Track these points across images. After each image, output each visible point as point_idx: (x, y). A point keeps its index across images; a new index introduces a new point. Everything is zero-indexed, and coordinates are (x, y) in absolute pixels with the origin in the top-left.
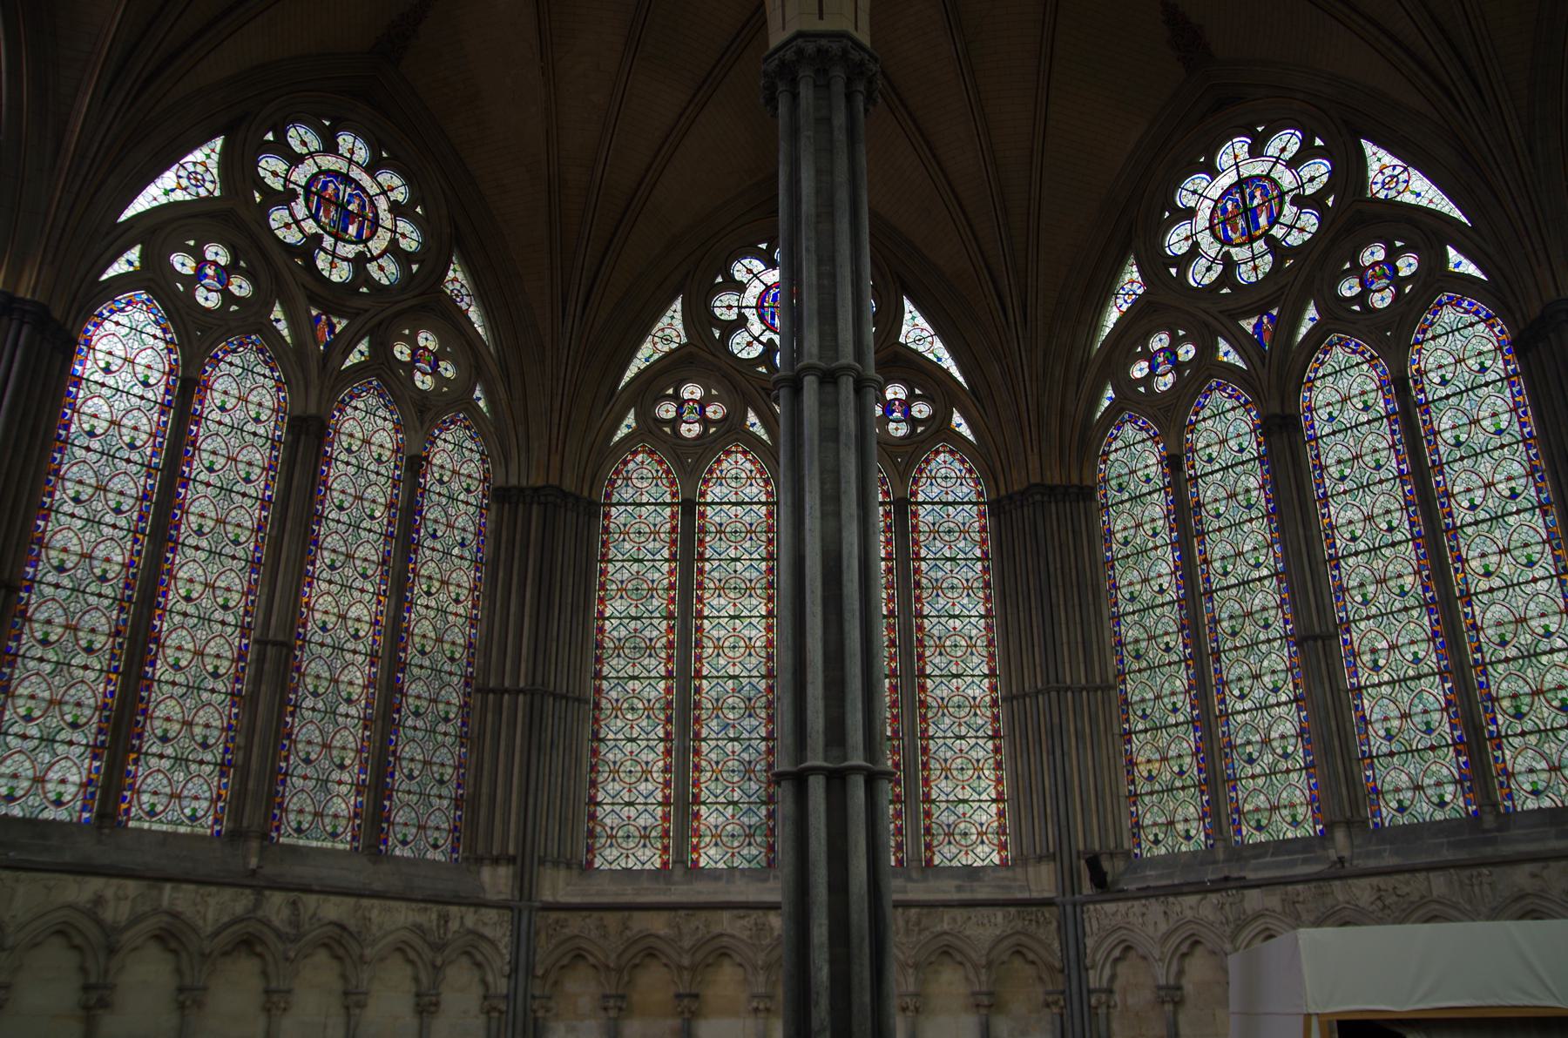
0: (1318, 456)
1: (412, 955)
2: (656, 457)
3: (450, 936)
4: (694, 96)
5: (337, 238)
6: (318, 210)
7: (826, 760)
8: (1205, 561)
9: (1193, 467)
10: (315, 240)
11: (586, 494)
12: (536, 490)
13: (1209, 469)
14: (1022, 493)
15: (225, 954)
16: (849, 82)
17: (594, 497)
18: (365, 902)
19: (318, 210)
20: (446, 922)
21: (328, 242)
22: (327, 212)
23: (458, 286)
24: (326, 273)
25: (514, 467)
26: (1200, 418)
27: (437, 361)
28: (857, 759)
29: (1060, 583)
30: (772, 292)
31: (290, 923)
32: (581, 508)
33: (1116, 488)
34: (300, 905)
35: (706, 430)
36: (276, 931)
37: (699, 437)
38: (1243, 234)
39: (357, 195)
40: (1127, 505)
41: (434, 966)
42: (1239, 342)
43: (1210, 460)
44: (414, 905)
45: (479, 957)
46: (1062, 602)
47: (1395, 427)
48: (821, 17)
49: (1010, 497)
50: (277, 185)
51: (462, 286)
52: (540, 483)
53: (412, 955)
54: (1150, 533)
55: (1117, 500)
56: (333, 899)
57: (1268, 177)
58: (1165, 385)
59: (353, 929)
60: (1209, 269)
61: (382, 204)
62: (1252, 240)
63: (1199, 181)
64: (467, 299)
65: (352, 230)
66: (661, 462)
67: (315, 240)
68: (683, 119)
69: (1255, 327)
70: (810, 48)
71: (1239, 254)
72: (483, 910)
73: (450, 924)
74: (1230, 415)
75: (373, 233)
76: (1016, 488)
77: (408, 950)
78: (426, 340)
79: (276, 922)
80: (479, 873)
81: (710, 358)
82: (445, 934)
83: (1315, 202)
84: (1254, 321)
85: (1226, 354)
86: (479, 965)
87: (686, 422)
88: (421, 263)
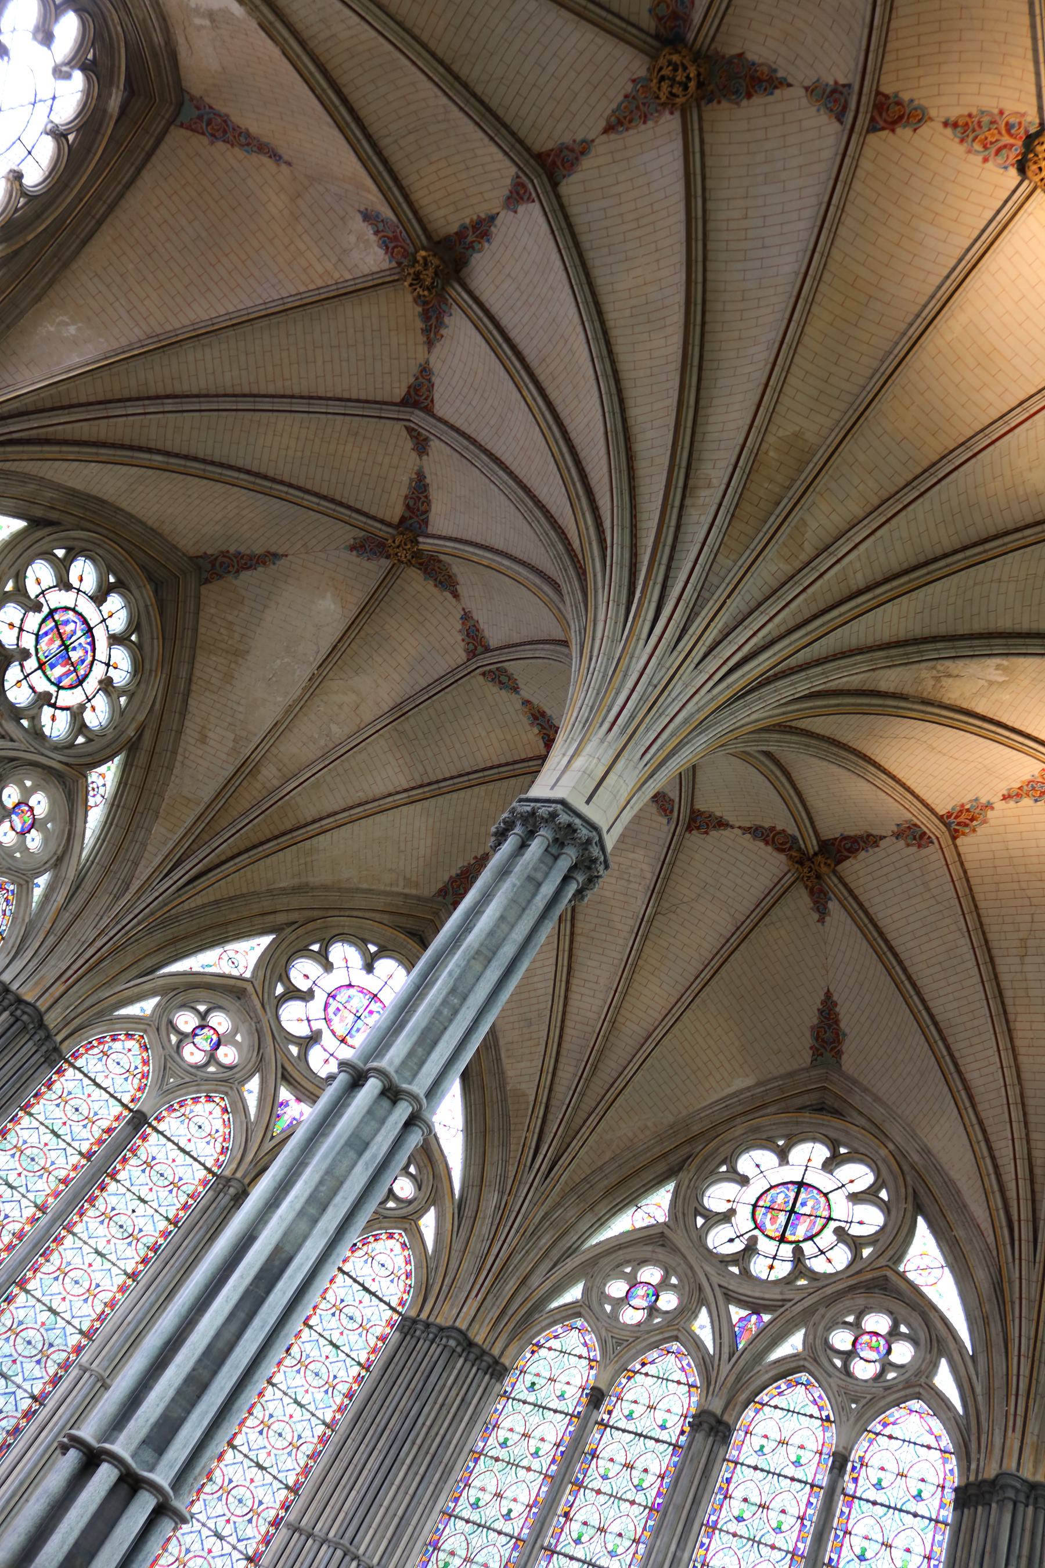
0: (729, 1481)
2: (145, 1055)
4: (413, 788)
5: (41, 666)
6: (46, 634)
7: (133, 1456)
8: (566, 1515)
9: (610, 1413)
10: (25, 654)
11: (59, 1038)
12: (19, 1001)
13: (622, 1424)
14: (441, 1329)
16: (574, 868)
17: (64, 1047)
19: (46, 634)
21: (31, 664)
22: (52, 641)
23: (100, 782)
25: (18, 965)
26: (644, 1370)
27: (32, 826)
28: (162, 1477)
29: (419, 1441)
32: (44, 1048)
33: (528, 1385)
35: (207, 1064)
37: (197, 1067)
38: (777, 1230)
39: (85, 648)
40: (529, 1408)
42: (720, 1322)
43: (629, 1417)
46: (408, 1461)
47: (813, 1500)
48: (588, 802)
49: (428, 1325)
50: (33, 590)
51: (104, 785)
52: (29, 998)
54: (532, 1450)
55: (521, 1396)
57: (826, 1195)
58: (632, 1318)
60: (731, 1240)
61: (98, 671)
62: (782, 1239)
63: (766, 1158)
64: (98, 798)
65: (58, 671)
66: (145, 1063)
67: (25, 654)
68: (390, 799)
69: (741, 1319)
70: (564, 818)
71: (765, 1245)
74: (672, 1386)
76: (438, 1321)
78: (40, 804)
81: (259, 1006)
83: (855, 1244)
84: (744, 1313)
85: (702, 1327)
87: (195, 1045)
88: (89, 740)
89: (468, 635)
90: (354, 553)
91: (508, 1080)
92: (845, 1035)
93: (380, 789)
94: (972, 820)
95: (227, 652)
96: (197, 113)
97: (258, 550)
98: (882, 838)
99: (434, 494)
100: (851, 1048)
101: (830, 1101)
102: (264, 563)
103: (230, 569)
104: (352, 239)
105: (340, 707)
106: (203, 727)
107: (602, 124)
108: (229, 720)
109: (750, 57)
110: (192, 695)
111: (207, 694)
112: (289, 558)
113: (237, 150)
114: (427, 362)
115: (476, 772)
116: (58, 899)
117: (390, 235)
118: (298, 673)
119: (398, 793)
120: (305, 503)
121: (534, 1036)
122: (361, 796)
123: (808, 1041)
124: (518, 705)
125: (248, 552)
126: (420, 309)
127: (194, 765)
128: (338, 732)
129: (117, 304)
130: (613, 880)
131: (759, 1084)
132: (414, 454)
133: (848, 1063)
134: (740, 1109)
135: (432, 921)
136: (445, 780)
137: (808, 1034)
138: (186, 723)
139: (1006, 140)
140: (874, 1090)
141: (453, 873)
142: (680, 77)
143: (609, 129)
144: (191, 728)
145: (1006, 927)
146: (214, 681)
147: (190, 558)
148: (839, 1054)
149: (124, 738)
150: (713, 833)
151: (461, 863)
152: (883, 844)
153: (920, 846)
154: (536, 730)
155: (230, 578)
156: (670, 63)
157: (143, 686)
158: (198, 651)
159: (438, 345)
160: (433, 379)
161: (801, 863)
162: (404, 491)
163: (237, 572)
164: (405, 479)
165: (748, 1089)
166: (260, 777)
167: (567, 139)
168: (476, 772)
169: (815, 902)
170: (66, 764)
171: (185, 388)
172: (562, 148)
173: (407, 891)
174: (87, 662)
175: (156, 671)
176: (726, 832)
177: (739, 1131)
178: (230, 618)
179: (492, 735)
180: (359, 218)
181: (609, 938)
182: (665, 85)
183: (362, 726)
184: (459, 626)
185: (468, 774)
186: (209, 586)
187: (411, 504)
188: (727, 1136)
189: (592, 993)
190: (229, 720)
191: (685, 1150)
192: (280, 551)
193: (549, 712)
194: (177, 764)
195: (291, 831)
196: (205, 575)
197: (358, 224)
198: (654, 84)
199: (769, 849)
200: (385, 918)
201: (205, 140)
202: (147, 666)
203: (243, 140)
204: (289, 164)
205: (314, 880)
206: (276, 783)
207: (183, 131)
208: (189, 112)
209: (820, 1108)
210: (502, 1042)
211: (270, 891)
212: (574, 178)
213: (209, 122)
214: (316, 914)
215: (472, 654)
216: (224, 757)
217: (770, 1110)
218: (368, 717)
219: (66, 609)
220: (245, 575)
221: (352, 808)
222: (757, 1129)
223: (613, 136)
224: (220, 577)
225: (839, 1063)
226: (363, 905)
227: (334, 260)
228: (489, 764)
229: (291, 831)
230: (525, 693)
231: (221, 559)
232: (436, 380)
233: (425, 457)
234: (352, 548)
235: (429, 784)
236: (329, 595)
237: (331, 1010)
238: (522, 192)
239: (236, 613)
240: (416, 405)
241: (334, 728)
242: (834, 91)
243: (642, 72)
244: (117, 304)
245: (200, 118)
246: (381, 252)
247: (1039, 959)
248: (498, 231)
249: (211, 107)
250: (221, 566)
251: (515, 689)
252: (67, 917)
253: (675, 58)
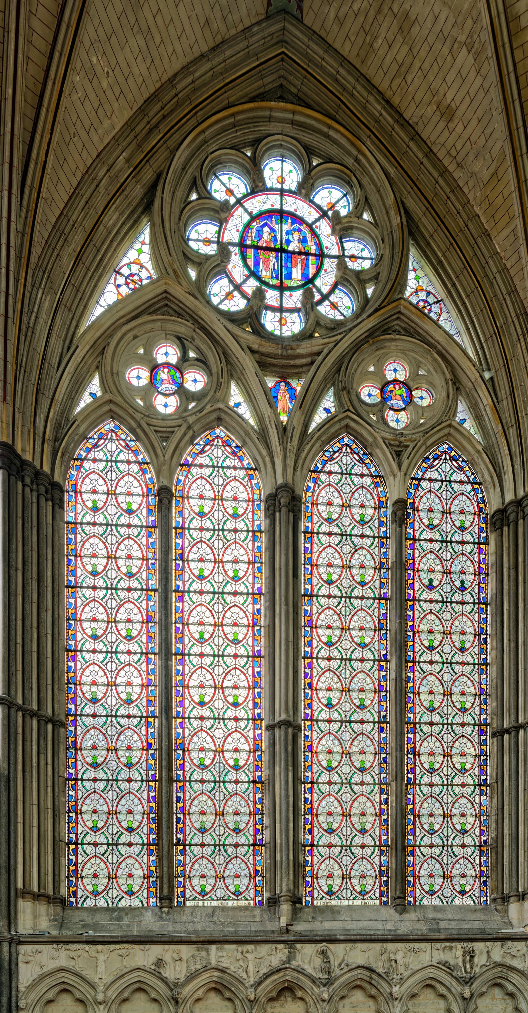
1: (442, 990)
3: (477, 970)
5: (281, 288)
6: (257, 264)
15: (271, 1000)
18: (391, 946)
19: (257, 264)
20: (472, 957)
21: (272, 297)
22: (267, 261)
24: (277, 333)
25: (508, 479)
31: (322, 970)
34: (329, 953)
36: (309, 977)
39: (294, 230)
41: (464, 999)
44: (438, 945)
45: (510, 988)
53: (442, 990)
56: (360, 946)
59: (381, 971)
72: (510, 944)
73: (476, 959)
75: (319, 269)
77: (438, 986)
79: (309, 970)
80: (506, 911)
82: (472, 968)
86: (511, 995)
116: (485, 403)
147: (267, 18)
149: (397, 232)
157: (365, 181)
170: (376, 310)
174: (308, 236)
175: (359, 151)
202: (350, 161)
219: (247, 227)
252: (506, 404)
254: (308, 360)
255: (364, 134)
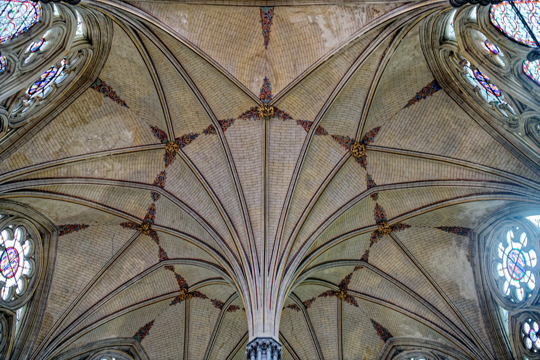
4: (99, 204)
30: (13, 250)
68: (91, 203)
89: (159, 178)
90: (151, 129)
91: (47, 308)
92: (148, 334)
93: (88, 197)
94: (233, 309)
95: (80, 117)
96: (267, 12)
97: (122, 98)
98: (207, 298)
99: (194, 142)
100: (147, 338)
101: (132, 351)
102: (119, 102)
103: (106, 93)
104: (257, 79)
105: (104, 167)
106: (50, 135)
107: (333, 134)
108: (63, 140)
109: (367, 158)
110: (55, 120)
111: (61, 124)
112: (129, 110)
113: (262, 30)
114: (235, 120)
115: (121, 211)
117: (266, 91)
118: (101, 146)
119: (94, 202)
120: (166, 115)
121: (67, 297)
122: (81, 195)
123: (137, 331)
124: (150, 203)
125: (118, 95)
126: (249, 110)
127: (36, 146)
128: (97, 174)
129: (200, 28)
130: (129, 264)
131: (117, 338)
132: (202, 131)
133: (143, 342)
134: (108, 344)
135: (49, 233)
136: (110, 208)
137: (139, 328)
138: (45, 128)
139: (380, 215)
140: (148, 355)
141: (71, 224)
142: (361, 153)
143: (333, 136)
144: (45, 132)
145: (222, 338)
146: (67, 122)
148: (143, 338)
150: (168, 270)
151: (77, 223)
152: (206, 299)
153: (216, 307)
154: (147, 212)
155: (102, 95)
156: (362, 148)
158: (70, 106)
159: (242, 120)
160: (232, 125)
161: (186, 294)
162: (187, 133)
163: (107, 96)
164: (191, 131)
165: (113, 339)
166: (59, 170)
167: (325, 129)
168: (121, 211)
169: (174, 300)
171: (184, 65)
172: (323, 129)
173: (52, 221)
176: (171, 272)
177: (105, 351)
178: (91, 106)
179: (134, 205)
180: (264, 78)
181: (115, 280)
182: (356, 150)
183: (106, 178)
184: (159, 173)
185: (118, 210)
186: (92, 90)
187: (185, 137)
188: (100, 352)
189: (98, 294)
190: (63, 140)
191: (88, 353)
192: (128, 105)
193: (157, 211)
194: (30, 141)
195: (51, 192)
196: (95, 85)
197: (262, 79)
198: (355, 147)
199: (177, 282)
200: (38, 226)
201: (260, 19)
203: (266, 30)
204: (266, 48)
205: (32, 205)
206: (62, 175)
207: (259, 11)
208: (266, 10)
209: (128, 352)
210: (50, 292)
211: (17, 202)
212: (318, 136)
213: (266, 18)
214: (21, 215)
215: (155, 184)
216: (51, 153)
217: (115, 347)
218: (109, 177)
220: (108, 99)
221: (76, 197)
222: (108, 353)
223: (332, 138)
224: (99, 91)
225: (141, 341)
226: (36, 218)
227: (249, 80)
228: (126, 211)
229: (51, 192)
230: (156, 203)
231: (106, 87)
232: (232, 126)
233: (204, 134)
234: (152, 127)
235: (105, 206)
236: (132, 132)
237: (3, 257)
238: (305, 124)
239: (94, 107)
240: (221, 125)
241: (96, 171)
242: (371, 181)
243: (351, 138)
244: (200, 28)
245: (266, 14)
246: (259, 91)
247: (224, 350)
248: (288, 122)
249: (272, 17)
250: (103, 88)
251: (155, 200)
253: (364, 149)
254: (8, 105)
255: (56, 105)
